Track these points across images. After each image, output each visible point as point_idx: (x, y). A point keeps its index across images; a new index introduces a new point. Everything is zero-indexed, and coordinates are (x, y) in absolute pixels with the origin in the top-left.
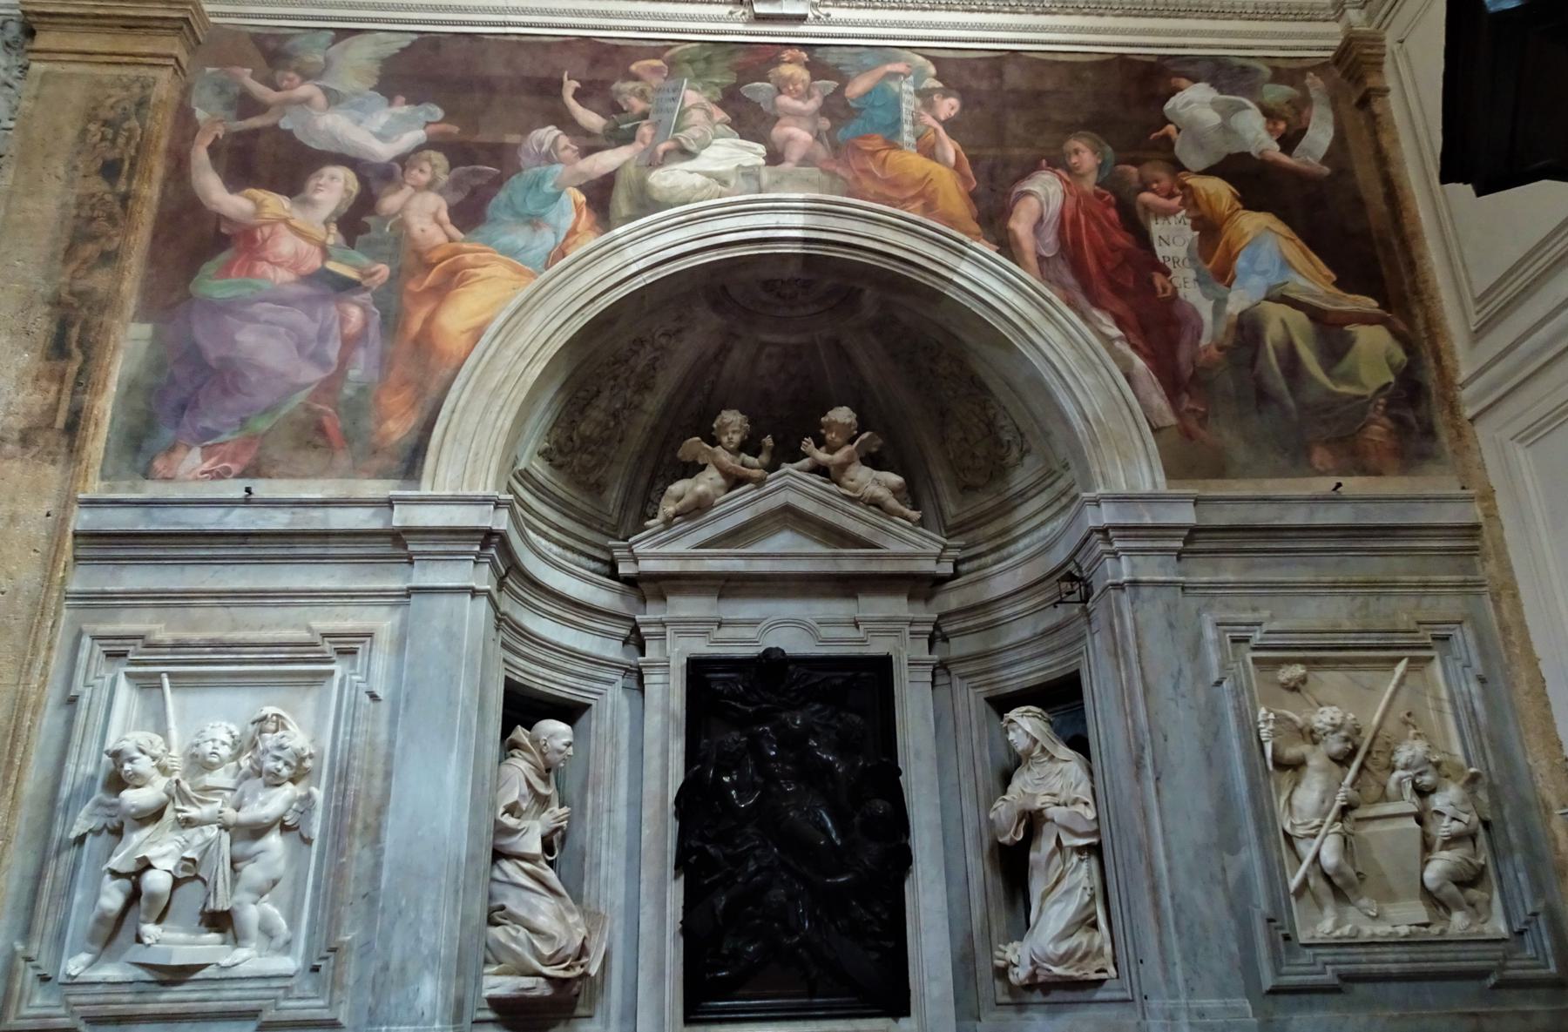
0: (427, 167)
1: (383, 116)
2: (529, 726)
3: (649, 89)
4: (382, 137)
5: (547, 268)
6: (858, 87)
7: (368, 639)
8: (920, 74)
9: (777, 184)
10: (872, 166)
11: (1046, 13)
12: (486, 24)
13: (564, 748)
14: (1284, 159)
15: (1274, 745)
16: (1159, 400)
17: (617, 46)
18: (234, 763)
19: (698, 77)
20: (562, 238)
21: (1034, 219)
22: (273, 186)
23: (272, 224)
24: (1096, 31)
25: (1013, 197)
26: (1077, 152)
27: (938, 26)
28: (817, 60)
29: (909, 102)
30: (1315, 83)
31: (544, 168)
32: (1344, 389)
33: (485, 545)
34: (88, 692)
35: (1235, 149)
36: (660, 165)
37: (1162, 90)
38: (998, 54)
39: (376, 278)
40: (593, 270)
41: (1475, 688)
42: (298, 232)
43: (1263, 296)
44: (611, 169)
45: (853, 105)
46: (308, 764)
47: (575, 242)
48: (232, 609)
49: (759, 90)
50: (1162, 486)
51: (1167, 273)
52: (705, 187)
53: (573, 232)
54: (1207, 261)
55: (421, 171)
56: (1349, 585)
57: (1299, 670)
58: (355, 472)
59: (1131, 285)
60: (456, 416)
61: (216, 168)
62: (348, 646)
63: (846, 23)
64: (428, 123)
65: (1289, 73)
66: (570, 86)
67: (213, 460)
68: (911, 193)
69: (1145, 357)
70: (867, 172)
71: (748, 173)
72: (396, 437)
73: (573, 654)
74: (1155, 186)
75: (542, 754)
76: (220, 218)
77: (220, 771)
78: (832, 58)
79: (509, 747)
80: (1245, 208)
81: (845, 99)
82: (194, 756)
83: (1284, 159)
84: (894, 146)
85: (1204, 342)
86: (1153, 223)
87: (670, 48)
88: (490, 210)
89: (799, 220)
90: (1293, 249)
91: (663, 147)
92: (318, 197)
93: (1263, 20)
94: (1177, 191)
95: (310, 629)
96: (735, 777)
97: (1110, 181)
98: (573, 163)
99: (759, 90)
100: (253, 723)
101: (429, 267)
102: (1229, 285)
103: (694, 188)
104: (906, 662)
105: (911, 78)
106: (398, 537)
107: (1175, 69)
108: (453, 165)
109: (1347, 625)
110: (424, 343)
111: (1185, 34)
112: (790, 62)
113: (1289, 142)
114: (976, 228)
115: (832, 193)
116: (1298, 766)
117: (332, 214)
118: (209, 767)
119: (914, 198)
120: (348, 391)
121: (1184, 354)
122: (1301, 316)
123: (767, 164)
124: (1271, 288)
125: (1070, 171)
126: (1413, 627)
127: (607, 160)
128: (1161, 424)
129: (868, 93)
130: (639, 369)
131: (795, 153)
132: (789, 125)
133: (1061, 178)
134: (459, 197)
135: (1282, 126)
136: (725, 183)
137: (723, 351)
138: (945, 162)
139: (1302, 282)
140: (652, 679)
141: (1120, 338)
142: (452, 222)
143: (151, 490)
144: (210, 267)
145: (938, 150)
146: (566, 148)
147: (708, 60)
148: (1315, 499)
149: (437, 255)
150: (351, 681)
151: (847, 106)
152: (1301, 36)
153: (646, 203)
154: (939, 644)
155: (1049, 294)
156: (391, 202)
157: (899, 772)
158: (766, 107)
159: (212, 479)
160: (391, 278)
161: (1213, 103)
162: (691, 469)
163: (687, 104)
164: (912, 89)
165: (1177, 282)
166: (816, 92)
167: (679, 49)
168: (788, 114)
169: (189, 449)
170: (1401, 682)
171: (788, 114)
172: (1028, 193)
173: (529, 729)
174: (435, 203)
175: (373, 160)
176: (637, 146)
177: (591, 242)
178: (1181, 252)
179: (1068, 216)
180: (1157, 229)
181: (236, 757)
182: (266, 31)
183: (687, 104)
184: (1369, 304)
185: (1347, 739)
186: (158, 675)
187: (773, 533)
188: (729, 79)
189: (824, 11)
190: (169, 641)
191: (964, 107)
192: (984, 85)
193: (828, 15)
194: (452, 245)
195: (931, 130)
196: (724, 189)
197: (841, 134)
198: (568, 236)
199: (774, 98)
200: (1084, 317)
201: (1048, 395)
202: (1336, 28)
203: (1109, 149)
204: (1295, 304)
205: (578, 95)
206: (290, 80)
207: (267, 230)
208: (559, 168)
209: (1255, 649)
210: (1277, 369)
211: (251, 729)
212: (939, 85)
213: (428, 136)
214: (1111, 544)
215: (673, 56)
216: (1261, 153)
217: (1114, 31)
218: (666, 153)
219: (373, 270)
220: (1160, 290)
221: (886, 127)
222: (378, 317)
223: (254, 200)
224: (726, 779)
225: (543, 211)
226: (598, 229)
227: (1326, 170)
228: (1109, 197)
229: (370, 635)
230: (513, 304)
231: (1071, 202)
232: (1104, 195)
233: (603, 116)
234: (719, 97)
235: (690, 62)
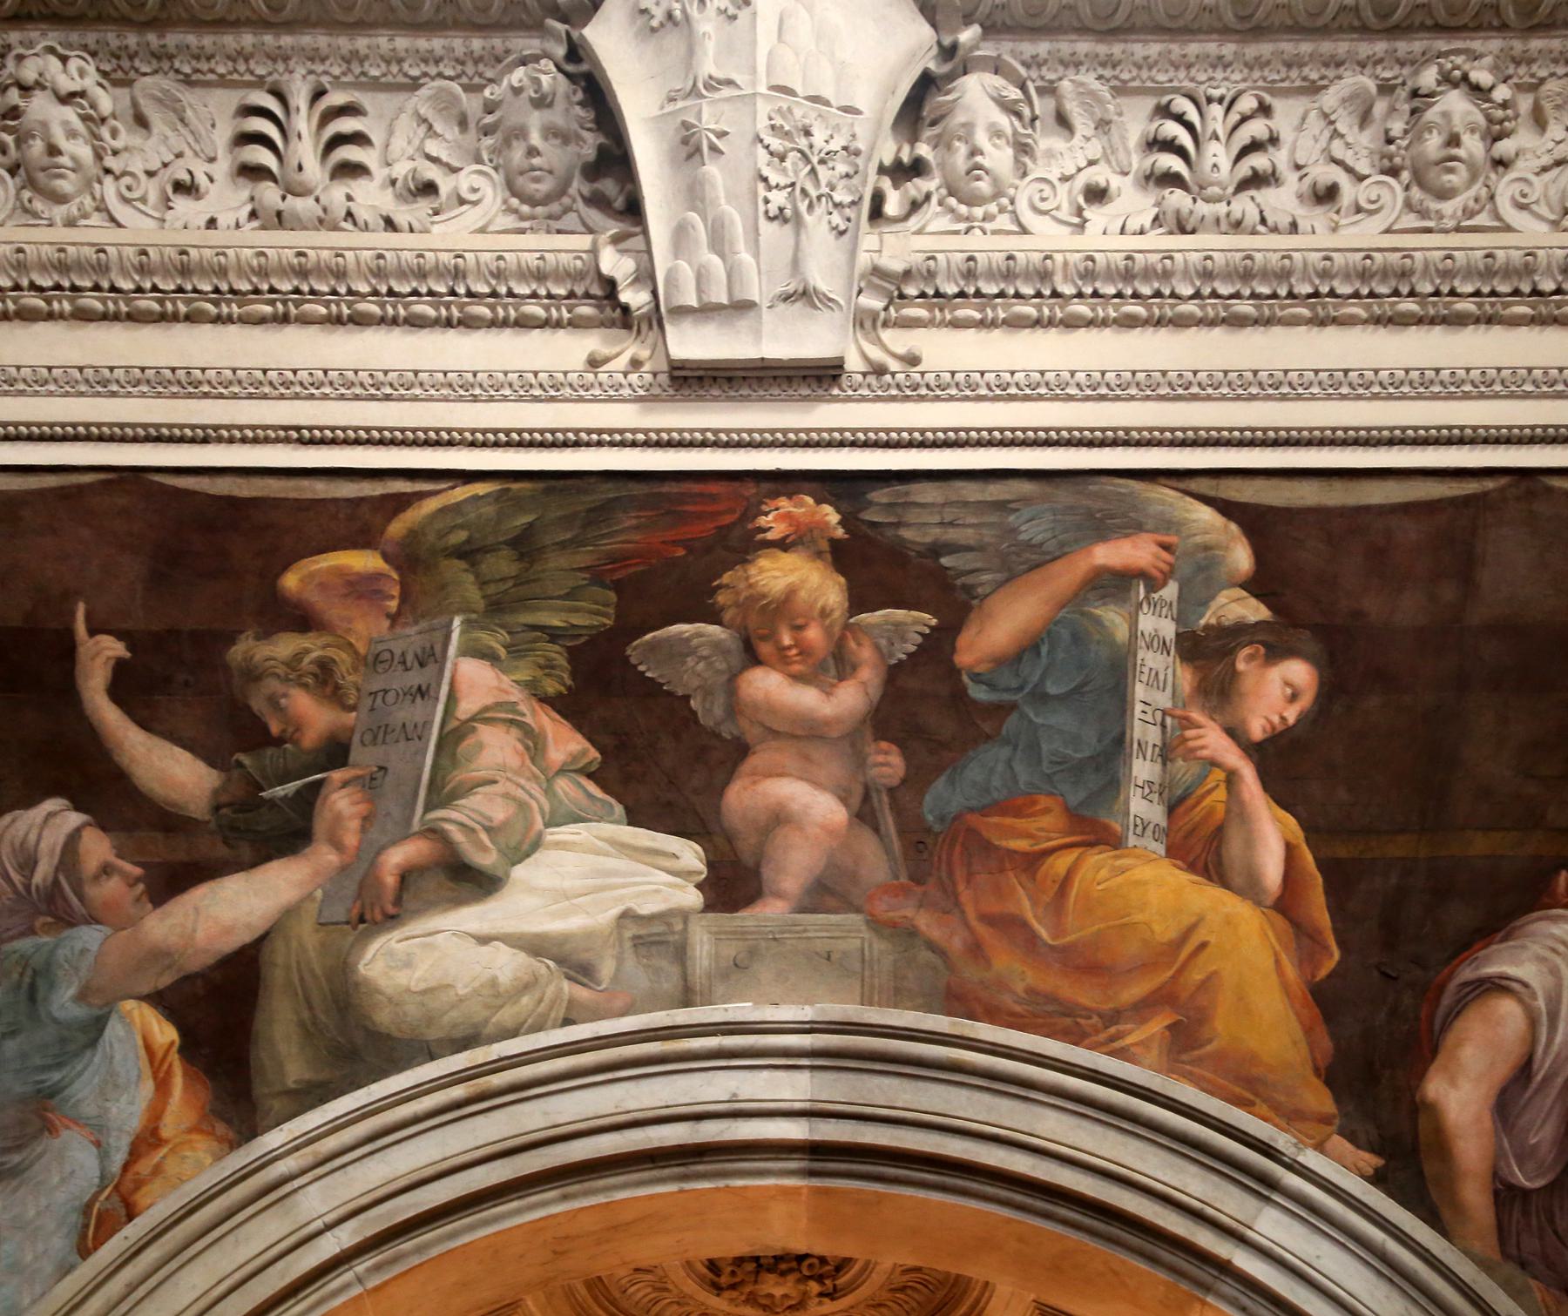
3: (343, 658)
5: (84, 1252)
10: (1025, 907)
19: (496, 607)
20: (119, 1158)
29: (1155, 682)
31: (46, 939)
36: (392, 920)
38: (1471, 487)
40: (211, 1256)
44: (246, 937)
45: (978, 693)
47: (157, 1170)
52: (526, 987)
53: (148, 1140)
63: (967, 388)
68: (1136, 990)
81: (954, 672)
91: (397, 857)
98: (133, 922)
103: (496, 995)
105: (1170, 591)
112: (783, 545)
115: (898, 997)
119: (1143, 1008)
123: (709, 907)
136: (581, 971)
138: (1250, 889)
145: (1234, 848)
146: (106, 870)
147: (524, 545)
151: (959, 696)
158: (709, 711)
163: (466, 708)
164: (1168, 629)
166: (866, 653)
167: (431, 505)
168: (775, 734)
171: (775, 734)
176: (322, 858)
183: (467, 707)
189: (898, 340)
191: (1331, 690)
193: (912, 360)
195: (1219, 775)
196: (582, 993)
198: (135, 1154)
199: (733, 678)
205: (123, 687)
208: (89, 937)
212: (1254, 611)
215: (414, 535)
218: (406, 876)
221: (1077, 770)
225: (56, 1076)
226: (221, 1128)
233: (211, 763)
235: (468, 554)
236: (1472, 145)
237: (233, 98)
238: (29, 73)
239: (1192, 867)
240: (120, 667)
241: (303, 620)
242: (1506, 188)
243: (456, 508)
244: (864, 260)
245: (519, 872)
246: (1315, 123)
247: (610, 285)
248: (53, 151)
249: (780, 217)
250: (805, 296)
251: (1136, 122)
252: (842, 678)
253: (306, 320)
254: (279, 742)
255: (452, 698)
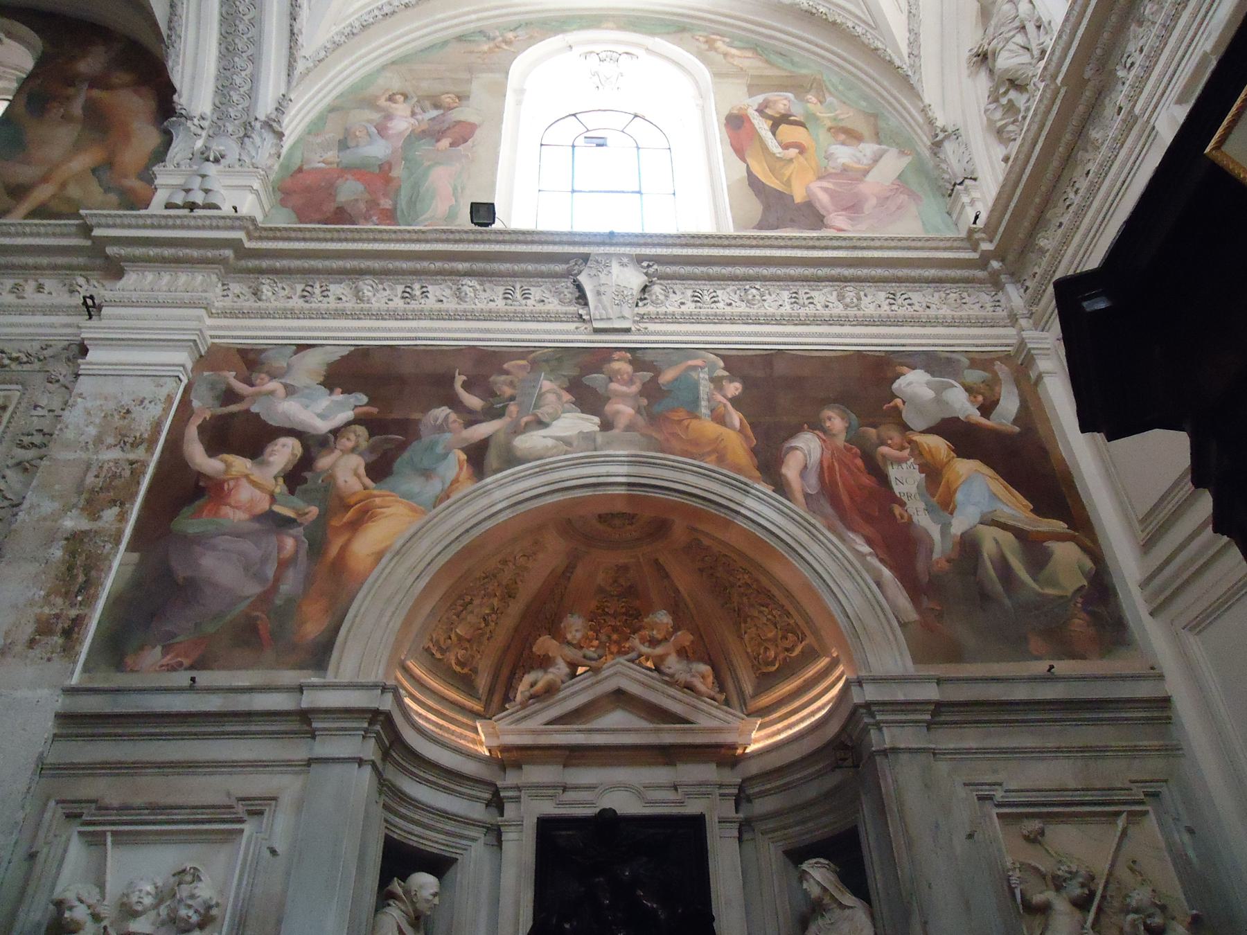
0: (352, 437)
1: (325, 401)
2: (404, 878)
3: (516, 380)
4: (322, 416)
5: (434, 507)
6: (667, 376)
7: (273, 803)
8: (713, 367)
9: (608, 444)
11: (802, 325)
12: (402, 339)
13: (431, 898)
14: (983, 421)
15: (1021, 890)
16: (903, 600)
17: (494, 352)
18: (155, 911)
21: (800, 466)
22: (241, 452)
23: (237, 479)
24: (839, 336)
25: (783, 452)
26: (830, 419)
27: (724, 334)
28: (638, 358)
30: (1002, 370)
32: (1049, 591)
33: (372, 722)
34: (45, 850)
35: (947, 416)
37: (890, 375)
38: (769, 352)
39: (307, 516)
41: (1186, 837)
42: (254, 484)
43: (978, 520)
44: (486, 436)
46: (214, 912)
47: (457, 488)
48: (171, 778)
49: (596, 379)
50: (910, 668)
51: (903, 504)
52: (555, 447)
53: (456, 480)
54: (933, 496)
55: (348, 439)
56: (1070, 750)
57: (1036, 825)
58: (279, 665)
59: (877, 513)
60: (358, 619)
61: (202, 441)
62: (257, 807)
63: (658, 333)
64: (356, 406)
65: (981, 361)
66: (459, 380)
67: (169, 657)
68: (708, 449)
69: (891, 568)
70: (674, 435)
71: (588, 437)
72: (312, 636)
73: (445, 815)
74: (889, 442)
75: (413, 903)
76: (200, 475)
77: (142, 919)
78: (649, 357)
79: (385, 897)
80: (959, 456)
82: (123, 904)
83: (983, 421)
84: (697, 417)
85: (936, 556)
86: (890, 468)
87: (533, 352)
88: (397, 465)
89: (624, 469)
90: (997, 485)
91: (525, 419)
92: (271, 459)
93: (959, 326)
94: (907, 445)
95: (229, 794)
96: (575, 923)
97: (854, 439)
99: (596, 379)
100: (174, 875)
101: (348, 507)
102: (951, 513)
103: (547, 448)
104: (717, 820)
105: (706, 369)
106: (305, 716)
107: (899, 361)
108: (371, 435)
109: (1072, 785)
110: (339, 566)
111: (903, 337)
112: (618, 360)
113: (987, 409)
114: (757, 474)
115: (648, 450)
116: (1044, 909)
117: (279, 473)
118: (135, 914)
119: (709, 453)
120: (278, 602)
121: (921, 565)
122: (1009, 536)
123: (601, 431)
124: (983, 515)
125: (825, 431)
126: (1128, 785)
127: (483, 430)
128: (906, 621)
129: (676, 380)
130: (504, 583)
131: (622, 422)
132: (619, 403)
133: (819, 437)
134: (373, 457)
135: (980, 398)
137: (570, 568)
138: (732, 427)
139: (1006, 509)
140: (509, 836)
141: (870, 554)
142: (367, 475)
143: (120, 680)
144: (187, 511)
145: (727, 419)
146: (455, 421)
147: (560, 360)
148: (1033, 679)
149: (352, 500)
150: (257, 838)
152: (986, 337)
153: (511, 459)
154: (744, 806)
155: (813, 521)
156: (324, 462)
157: (713, 919)
158: (601, 391)
159: (168, 670)
160: (319, 516)
161: (928, 384)
162: (545, 662)
163: (543, 390)
164: (707, 377)
165: (911, 510)
169: (154, 647)
170: (1124, 833)
172: (796, 448)
173: (404, 882)
174: (357, 462)
175: (315, 433)
177: (468, 487)
178: (913, 489)
179: (825, 465)
180: (893, 472)
181: (156, 906)
182: (250, 347)
183: (543, 390)
184: (1060, 526)
185: (1083, 885)
186: (104, 833)
187: (607, 711)
188: (574, 372)
190: (116, 803)
191: (745, 388)
192: (760, 374)
193: (646, 328)
194: (367, 491)
195: (721, 405)
196: (569, 449)
197: (657, 409)
198: (451, 484)
199: (607, 385)
200: (843, 539)
201: (818, 600)
202: (1012, 331)
203: (853, 416)
204: (1004, 527)
206: (262, 379)
207: (232, 483)
208: (448, 435)
209: (999, 805)
210: (992, 572)
211: (172, 880)
212: (726, 374)
213: (355, 415)
214: (874, 717)
216: (966, 418)
217: (852, 336)
218: (526, 424)
219: (306, 511)
220: (898, 517)
222: (307, 545)
223: (225, 462)
224: (567, 926)
227: (1017, 429)
228: (856, 450)
229: (274, 799)
230: (407, 535)
231: (828, 454)
232: (852, 449)
234: (566, 385)
235: (547, 361)
236: (758, 297)
237: (504, 288)
238: (464, 283)
239: (717, 423)
240: (464, 382)
241: (507, 373)
242: (766, 304)
243: (544, 353)
244: (635, 312)
245: (554, 423)
246: (725, 293)
247: (581, 316)
248: (466, 294)
249: (618, 304)
250: (623, 317)
251: (689, 293)
252: (632, 385)
253: (515, 321)
254: (499, 396)
255: (541, 388)
